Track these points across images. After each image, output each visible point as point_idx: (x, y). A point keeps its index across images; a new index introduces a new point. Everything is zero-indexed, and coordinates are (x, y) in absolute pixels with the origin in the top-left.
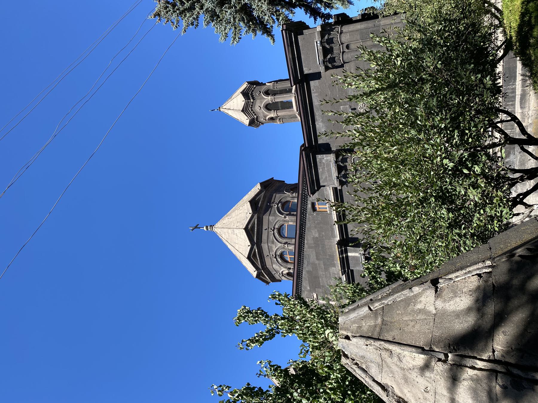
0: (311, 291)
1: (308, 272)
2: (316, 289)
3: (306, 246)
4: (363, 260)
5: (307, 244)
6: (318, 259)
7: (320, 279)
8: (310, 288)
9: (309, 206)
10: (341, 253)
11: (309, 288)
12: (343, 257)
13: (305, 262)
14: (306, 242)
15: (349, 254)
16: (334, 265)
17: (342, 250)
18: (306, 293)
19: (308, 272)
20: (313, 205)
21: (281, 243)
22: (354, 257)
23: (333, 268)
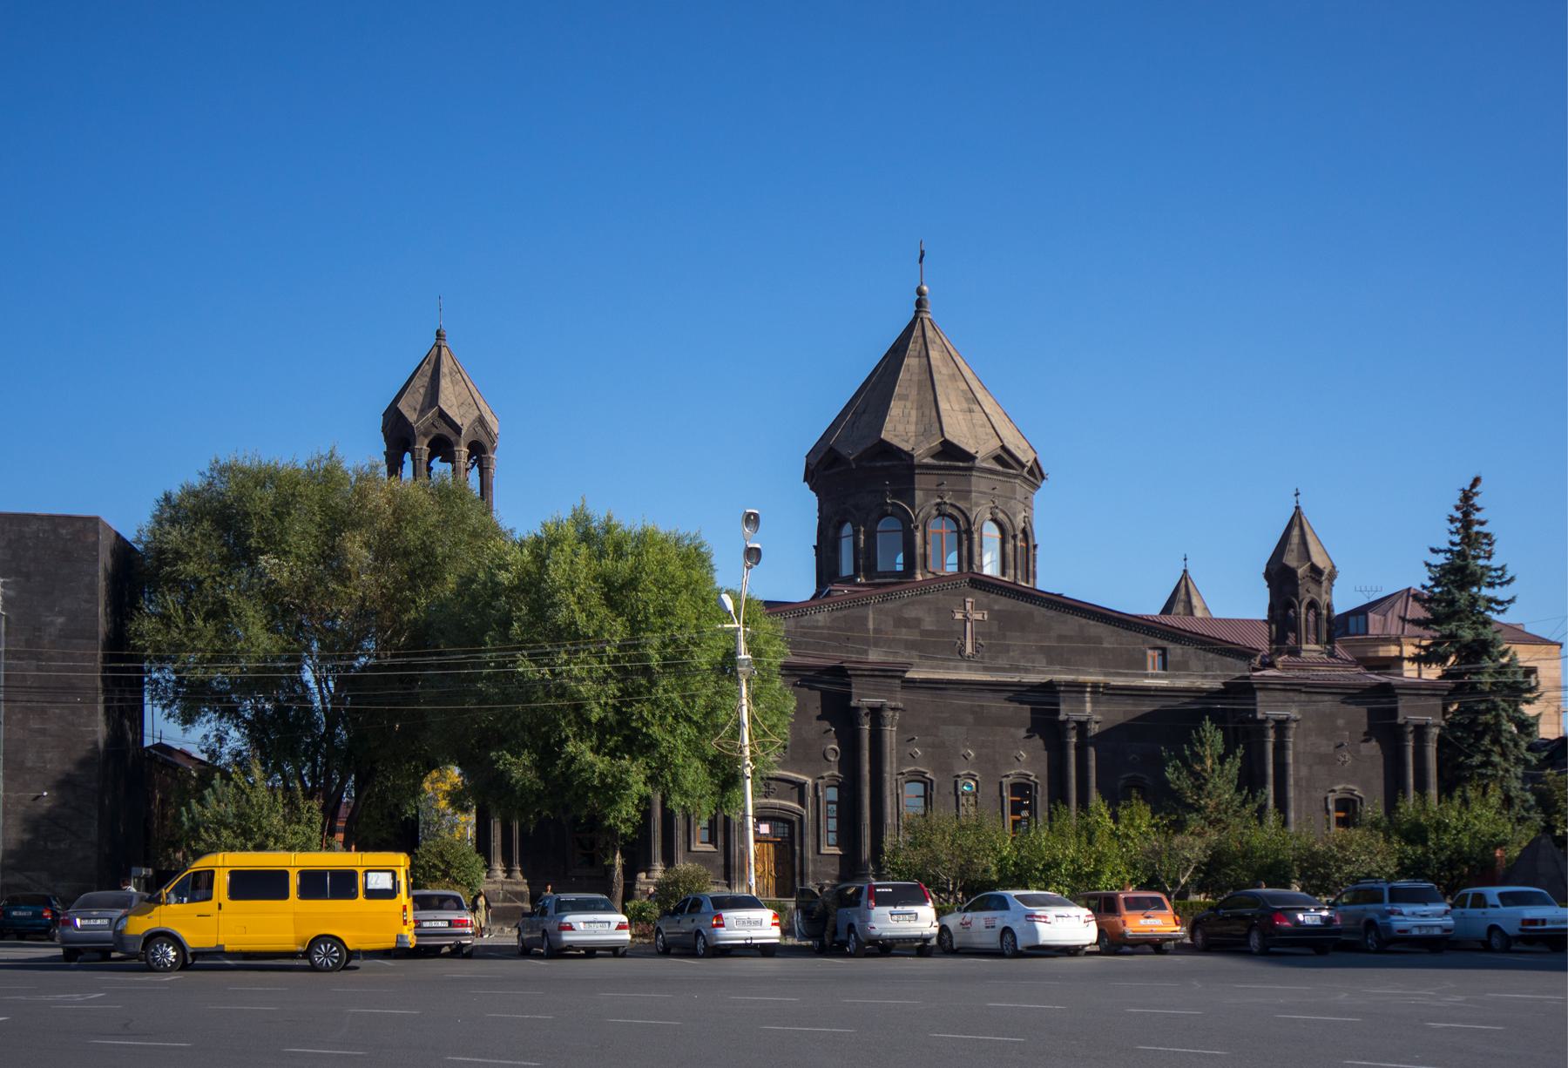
0: (991, 611)
2: (996, 622)
3: (1084, 621)
6: (1061, 638)
7: (1018, 634)
8: (999, 611)
10: (1095, 686)
11: (996, 607)
12: (1086, 687)
13: (1052, 613)
14: (1092, 622)
15: (1088, 695)
16: (1050, 662)
17: (1099, 687)
18: (985, 601)
23: (1045, 661)
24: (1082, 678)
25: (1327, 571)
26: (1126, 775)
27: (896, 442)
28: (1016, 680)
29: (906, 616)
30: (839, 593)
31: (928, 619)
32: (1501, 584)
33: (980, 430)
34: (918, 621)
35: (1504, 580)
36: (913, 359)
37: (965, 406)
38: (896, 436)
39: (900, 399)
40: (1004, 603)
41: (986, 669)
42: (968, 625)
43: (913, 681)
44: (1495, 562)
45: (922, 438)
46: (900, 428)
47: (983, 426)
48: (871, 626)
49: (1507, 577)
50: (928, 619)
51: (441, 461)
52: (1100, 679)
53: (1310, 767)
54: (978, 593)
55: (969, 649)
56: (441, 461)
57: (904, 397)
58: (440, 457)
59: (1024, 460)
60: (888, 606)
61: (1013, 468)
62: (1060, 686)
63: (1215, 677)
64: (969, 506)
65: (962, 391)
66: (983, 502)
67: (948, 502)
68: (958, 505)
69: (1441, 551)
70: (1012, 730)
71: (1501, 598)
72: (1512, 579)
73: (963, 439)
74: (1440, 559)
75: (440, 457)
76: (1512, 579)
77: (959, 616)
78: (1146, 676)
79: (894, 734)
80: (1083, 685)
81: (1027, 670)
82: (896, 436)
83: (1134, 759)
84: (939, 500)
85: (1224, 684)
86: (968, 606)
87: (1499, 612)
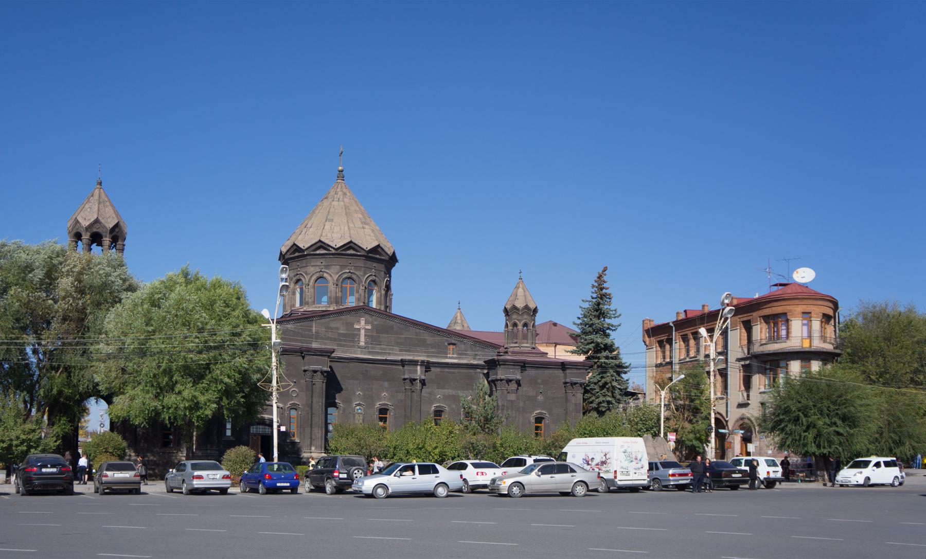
0: (372, 324)
1: (392, 327)
3: (418, 330)
4: (416, 378)
5: (420, 332)
8: (377, 324)
9: (453, 342)
10: (423, 362)
11: (376, 323)
14: (422, 331)
16: (401, 350)
18: (370, 319)
19: (392, 327)
20: (454, 344)
21: (365, 282)
22: (417, 370)
24: (416, 358)
25: (533, 309)
26: (436, 405)
27: (327, 242)
28: (384, 358)
29: (332, 326)
30: (296, 315)
31: (342, 328)
32: (615, 317)
33: (368, 238)
34: (337, 328)
35: (616, 315)
36: (336, 202)
37: (361, 225)
38: (327, 239)
39: (329, 221)
40: (379, 321)
41: (370, 353)
42: (363, 332)
43: (334, 358)
44: (612, 307)
45: (340, 240)
46: (329, 235)
47: (370, 235)
48: (314, 331)
49: (618, 314)
50: (342, 328)
51: (97, 245)
52: (425, 359)
53: (525, 402)
54: (368, 317)
55: (362, 344)
56: (97, 245)
57: (332, 220)
58: (96, 244)
59: (389, 253)
60: (323, 321)
61: (383, 256)
62: (406, 361)
63: (479, 359)
64: (361, 274)
65: (360, 218)
66: (368, 272)
67: (351, 271)
68: (357, 273)
69: (587, 301)
70: (381, 382)
71: (614, 324)
72: (620, 315)
73: (360, 241)
74: (586, 305)
75: (96, 244)
76: (620, 315)
77: (357, 327)
78: (447, 358)
79: (324, 384)
80: (417, 361)
81: (389, 354)
82: (327, 239)
83: (440, 397)
84: (348, 271)
85: (484, 362)
86: (363, 322)
87: (613, 330)
